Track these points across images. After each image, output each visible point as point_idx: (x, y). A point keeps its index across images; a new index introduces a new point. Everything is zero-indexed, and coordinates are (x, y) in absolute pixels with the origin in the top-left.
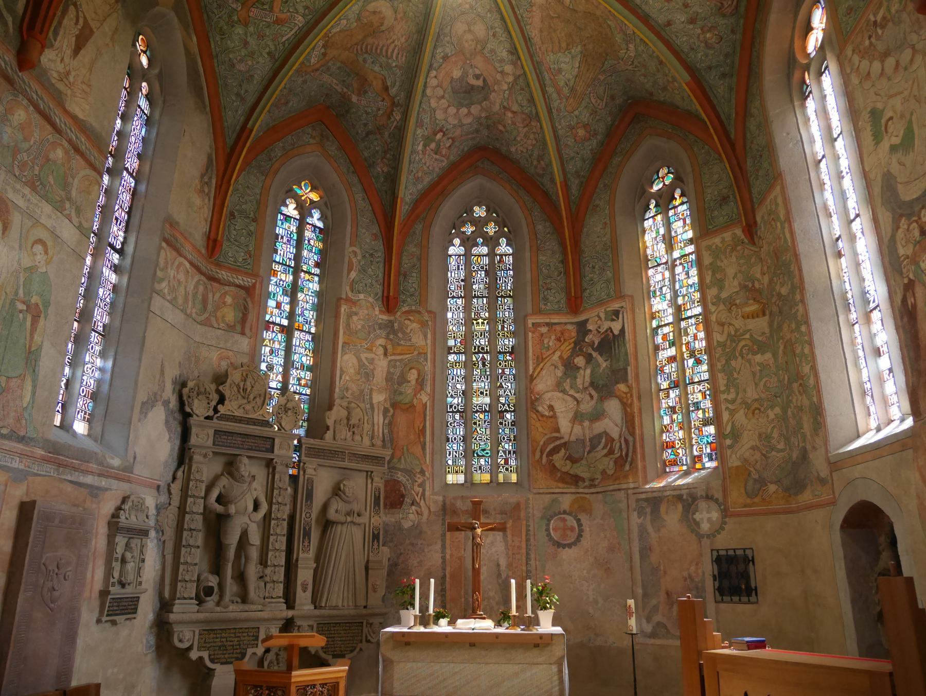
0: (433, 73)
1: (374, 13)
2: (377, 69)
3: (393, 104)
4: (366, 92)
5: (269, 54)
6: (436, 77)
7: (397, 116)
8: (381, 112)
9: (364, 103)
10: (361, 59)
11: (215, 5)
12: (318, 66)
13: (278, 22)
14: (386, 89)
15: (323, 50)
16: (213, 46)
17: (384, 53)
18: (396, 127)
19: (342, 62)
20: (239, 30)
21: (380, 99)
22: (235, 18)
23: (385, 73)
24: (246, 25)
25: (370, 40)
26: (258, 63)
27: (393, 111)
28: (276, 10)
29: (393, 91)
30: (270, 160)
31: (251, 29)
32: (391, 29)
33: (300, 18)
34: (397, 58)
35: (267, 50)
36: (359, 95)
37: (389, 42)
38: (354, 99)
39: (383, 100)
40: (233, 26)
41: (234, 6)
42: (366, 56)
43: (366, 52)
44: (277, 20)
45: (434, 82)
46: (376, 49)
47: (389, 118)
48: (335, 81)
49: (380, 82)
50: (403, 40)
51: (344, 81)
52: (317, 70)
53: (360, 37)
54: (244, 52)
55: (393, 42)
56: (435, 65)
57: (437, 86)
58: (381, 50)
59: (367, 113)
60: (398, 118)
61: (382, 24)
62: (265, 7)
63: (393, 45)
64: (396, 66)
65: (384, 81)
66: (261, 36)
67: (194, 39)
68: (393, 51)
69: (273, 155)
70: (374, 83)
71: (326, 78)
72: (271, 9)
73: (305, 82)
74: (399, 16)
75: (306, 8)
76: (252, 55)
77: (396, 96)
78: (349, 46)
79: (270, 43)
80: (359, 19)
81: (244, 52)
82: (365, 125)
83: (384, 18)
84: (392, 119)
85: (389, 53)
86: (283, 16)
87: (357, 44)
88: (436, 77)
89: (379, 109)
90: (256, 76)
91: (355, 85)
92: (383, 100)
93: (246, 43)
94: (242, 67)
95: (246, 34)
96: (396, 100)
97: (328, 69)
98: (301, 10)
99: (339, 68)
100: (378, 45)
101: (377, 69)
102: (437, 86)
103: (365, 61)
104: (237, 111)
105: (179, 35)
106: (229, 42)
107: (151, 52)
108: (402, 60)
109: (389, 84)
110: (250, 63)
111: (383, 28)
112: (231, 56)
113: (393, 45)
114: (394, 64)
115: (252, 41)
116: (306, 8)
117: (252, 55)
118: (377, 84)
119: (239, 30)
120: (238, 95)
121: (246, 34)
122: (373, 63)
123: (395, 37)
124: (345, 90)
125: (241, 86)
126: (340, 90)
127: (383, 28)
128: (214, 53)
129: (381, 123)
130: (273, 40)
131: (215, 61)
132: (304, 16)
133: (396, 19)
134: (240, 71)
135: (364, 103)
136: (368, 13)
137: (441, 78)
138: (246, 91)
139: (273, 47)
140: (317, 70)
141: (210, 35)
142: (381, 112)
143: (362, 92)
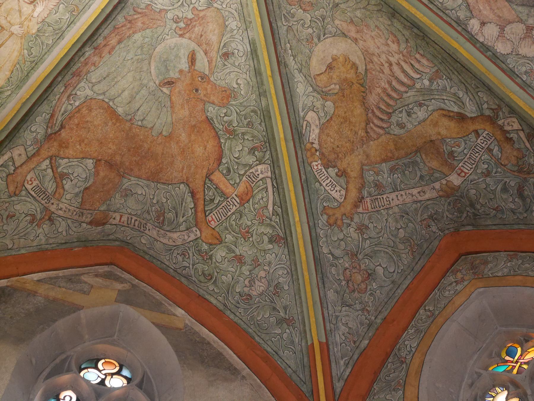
0: (474, 25)
1: (330, 67)
2: (421, 114)
3: (492, 120)
4: (451, 153)
5: (270, 241)
6: (483, 24)
7: (513, 124)
8: (496, 150)
9: (467, 169)
10: (397, 131)
11: (180, 258)
12: (353, 194)
13: (244, 199)
14: (461, 118)
15: (332, 172)
16: (214, 301)
17: (402, 89)
18: (529, 137)
19: (384, 161)
20: (220, 253)
21: (473, 137)
22: (205, 247)
23: (433, 105)
24: (221, 241)
25: (372, 99)
26: (270, 263)
27: (501, 128)
28: (229, 190)
29: (471, 110)
30: (402, 362)
31: (229, 238)
32: (367, 54)
33: (260, 167)
34: (417, 71)
35: (266, 239)
36: (452, 168)
37: (387, 70)
38: (455, 180)
39: (478, 135)
40: (211, 258)
41: (192, 237)
42: (394, 119)
43: (389, 115)
44: (241, 199)
45: (489, 34)
46: (389, 96)
47: (510, 140)
48: (415, 191)
49: (445, 122)
50: (394, 47)
51: (422, 177)
52: (361, 199)
53: (359, 110)
54: (245, 270)
55: (391, 65)
56: (462, 14)
57: (502, 29)
58: (395, 90)
59: (488, 174)
60: (516, 126)
61: (354, 66)
62: (216, 201)
63: (395, 68)
64: (431, 80)
65: (448, 115)
66: (246, 234)
67: (180, 312)
68: (404, 71)
69: (403, 354)
70: (444, 132)
71: (395, 199)
72: (224, 195)
73: (362, 228)
74: (353, 34)
75: (252, 151)
76: (256, 263)
77: (480, 107)
78: (362, 133)
79: (262, 229)
80: (324, 95)
81: (245, 270)
82: (505, 189)
83: (347, 59)
84: (513, 135)
85: (405, 80)
86: (242, 188)
87: (368, 122)
88: (483, 24)
89: (490, 150)
90: (281, 280)
91: (434, 164)
92: (478, 135)
93: (240, 259)
94: (260, 287)
95: (231, 251)
96: (487, 113)
97: (378, 186)
98: (251, 160)
99: (392, 170)
100: (384, 90)
101: (421, 114)
102: (502, 29)
103: (401, 126)
104: (293, 342)
105: (142, 320)
106: (224, 277)
107: (130, 368)
108: (425, 65)
109: (456, 109)
110: (262, 274)
111: (361, 69)
112: (238, 290)
113: (395, 68)
114: (426, 82)
115: (244, 249)
116: (252, 151)
117: (256, 263)
118: (447, 128)
119: (220, 253)
120: (280, 322)
121: (231, 251)
122: (409, 114)
123: (383, 58)
124: (437, 185)
125: (274, 309)
126: (434, 194)
127: (361, 69)
128: (221, 307)
129: (514, 160)
130: (262, 223)
131: (228, 313)
132: (260, 162)
133: (356, 40)
134: (261, 294)
135: (467, 169)
136: (324, 78)
137: (491, 16)
138: (285, 308)
139: (269, 230)
140: (361, 199)
141: (202, 292)
142: (496, 150)
143: (449, 160)
